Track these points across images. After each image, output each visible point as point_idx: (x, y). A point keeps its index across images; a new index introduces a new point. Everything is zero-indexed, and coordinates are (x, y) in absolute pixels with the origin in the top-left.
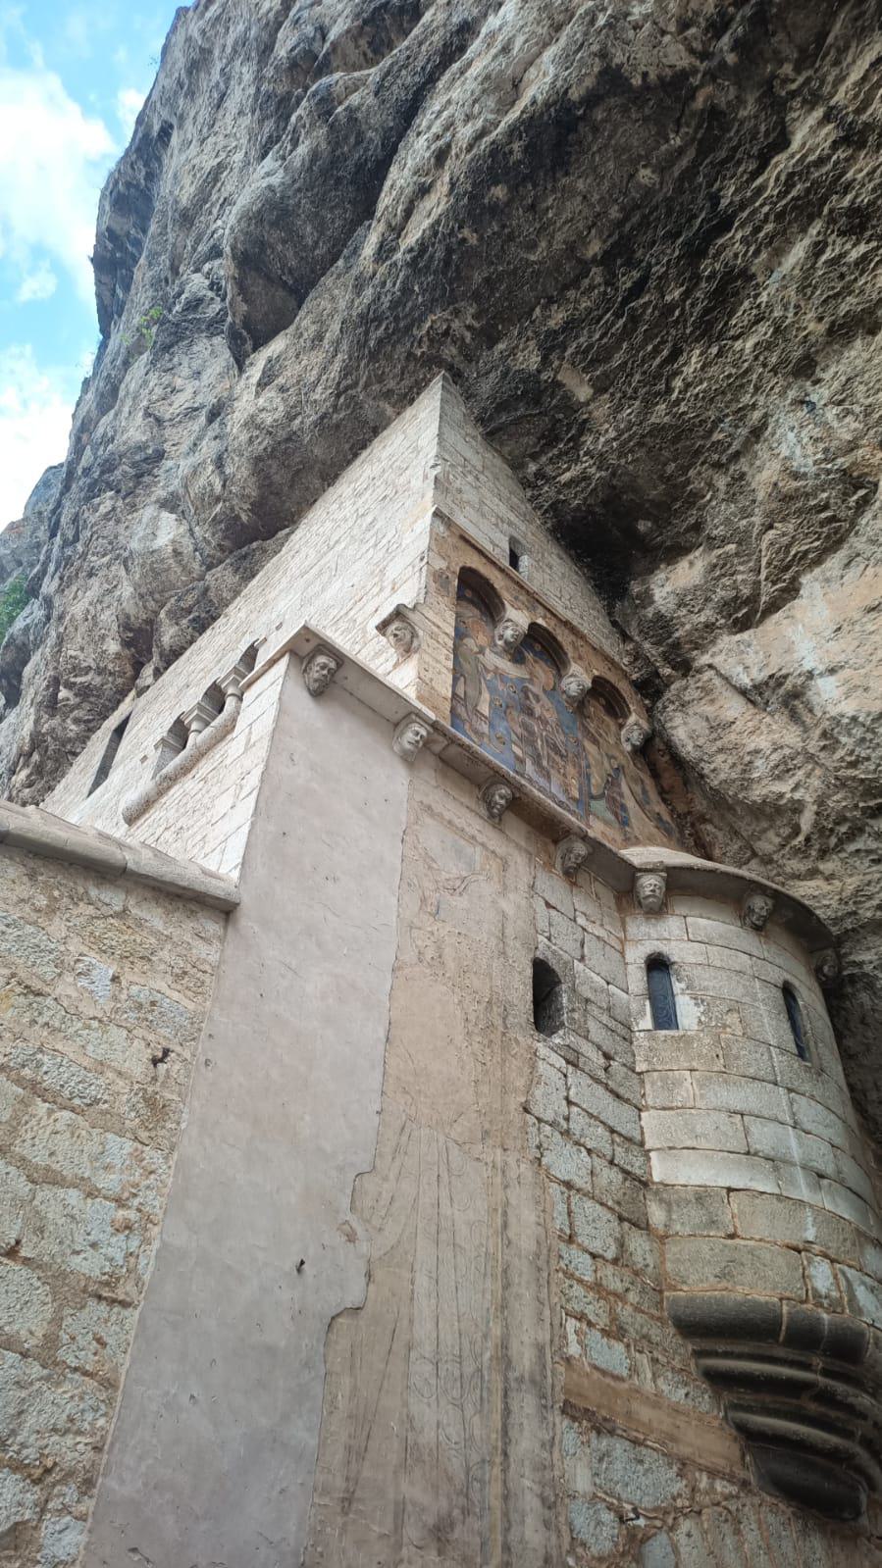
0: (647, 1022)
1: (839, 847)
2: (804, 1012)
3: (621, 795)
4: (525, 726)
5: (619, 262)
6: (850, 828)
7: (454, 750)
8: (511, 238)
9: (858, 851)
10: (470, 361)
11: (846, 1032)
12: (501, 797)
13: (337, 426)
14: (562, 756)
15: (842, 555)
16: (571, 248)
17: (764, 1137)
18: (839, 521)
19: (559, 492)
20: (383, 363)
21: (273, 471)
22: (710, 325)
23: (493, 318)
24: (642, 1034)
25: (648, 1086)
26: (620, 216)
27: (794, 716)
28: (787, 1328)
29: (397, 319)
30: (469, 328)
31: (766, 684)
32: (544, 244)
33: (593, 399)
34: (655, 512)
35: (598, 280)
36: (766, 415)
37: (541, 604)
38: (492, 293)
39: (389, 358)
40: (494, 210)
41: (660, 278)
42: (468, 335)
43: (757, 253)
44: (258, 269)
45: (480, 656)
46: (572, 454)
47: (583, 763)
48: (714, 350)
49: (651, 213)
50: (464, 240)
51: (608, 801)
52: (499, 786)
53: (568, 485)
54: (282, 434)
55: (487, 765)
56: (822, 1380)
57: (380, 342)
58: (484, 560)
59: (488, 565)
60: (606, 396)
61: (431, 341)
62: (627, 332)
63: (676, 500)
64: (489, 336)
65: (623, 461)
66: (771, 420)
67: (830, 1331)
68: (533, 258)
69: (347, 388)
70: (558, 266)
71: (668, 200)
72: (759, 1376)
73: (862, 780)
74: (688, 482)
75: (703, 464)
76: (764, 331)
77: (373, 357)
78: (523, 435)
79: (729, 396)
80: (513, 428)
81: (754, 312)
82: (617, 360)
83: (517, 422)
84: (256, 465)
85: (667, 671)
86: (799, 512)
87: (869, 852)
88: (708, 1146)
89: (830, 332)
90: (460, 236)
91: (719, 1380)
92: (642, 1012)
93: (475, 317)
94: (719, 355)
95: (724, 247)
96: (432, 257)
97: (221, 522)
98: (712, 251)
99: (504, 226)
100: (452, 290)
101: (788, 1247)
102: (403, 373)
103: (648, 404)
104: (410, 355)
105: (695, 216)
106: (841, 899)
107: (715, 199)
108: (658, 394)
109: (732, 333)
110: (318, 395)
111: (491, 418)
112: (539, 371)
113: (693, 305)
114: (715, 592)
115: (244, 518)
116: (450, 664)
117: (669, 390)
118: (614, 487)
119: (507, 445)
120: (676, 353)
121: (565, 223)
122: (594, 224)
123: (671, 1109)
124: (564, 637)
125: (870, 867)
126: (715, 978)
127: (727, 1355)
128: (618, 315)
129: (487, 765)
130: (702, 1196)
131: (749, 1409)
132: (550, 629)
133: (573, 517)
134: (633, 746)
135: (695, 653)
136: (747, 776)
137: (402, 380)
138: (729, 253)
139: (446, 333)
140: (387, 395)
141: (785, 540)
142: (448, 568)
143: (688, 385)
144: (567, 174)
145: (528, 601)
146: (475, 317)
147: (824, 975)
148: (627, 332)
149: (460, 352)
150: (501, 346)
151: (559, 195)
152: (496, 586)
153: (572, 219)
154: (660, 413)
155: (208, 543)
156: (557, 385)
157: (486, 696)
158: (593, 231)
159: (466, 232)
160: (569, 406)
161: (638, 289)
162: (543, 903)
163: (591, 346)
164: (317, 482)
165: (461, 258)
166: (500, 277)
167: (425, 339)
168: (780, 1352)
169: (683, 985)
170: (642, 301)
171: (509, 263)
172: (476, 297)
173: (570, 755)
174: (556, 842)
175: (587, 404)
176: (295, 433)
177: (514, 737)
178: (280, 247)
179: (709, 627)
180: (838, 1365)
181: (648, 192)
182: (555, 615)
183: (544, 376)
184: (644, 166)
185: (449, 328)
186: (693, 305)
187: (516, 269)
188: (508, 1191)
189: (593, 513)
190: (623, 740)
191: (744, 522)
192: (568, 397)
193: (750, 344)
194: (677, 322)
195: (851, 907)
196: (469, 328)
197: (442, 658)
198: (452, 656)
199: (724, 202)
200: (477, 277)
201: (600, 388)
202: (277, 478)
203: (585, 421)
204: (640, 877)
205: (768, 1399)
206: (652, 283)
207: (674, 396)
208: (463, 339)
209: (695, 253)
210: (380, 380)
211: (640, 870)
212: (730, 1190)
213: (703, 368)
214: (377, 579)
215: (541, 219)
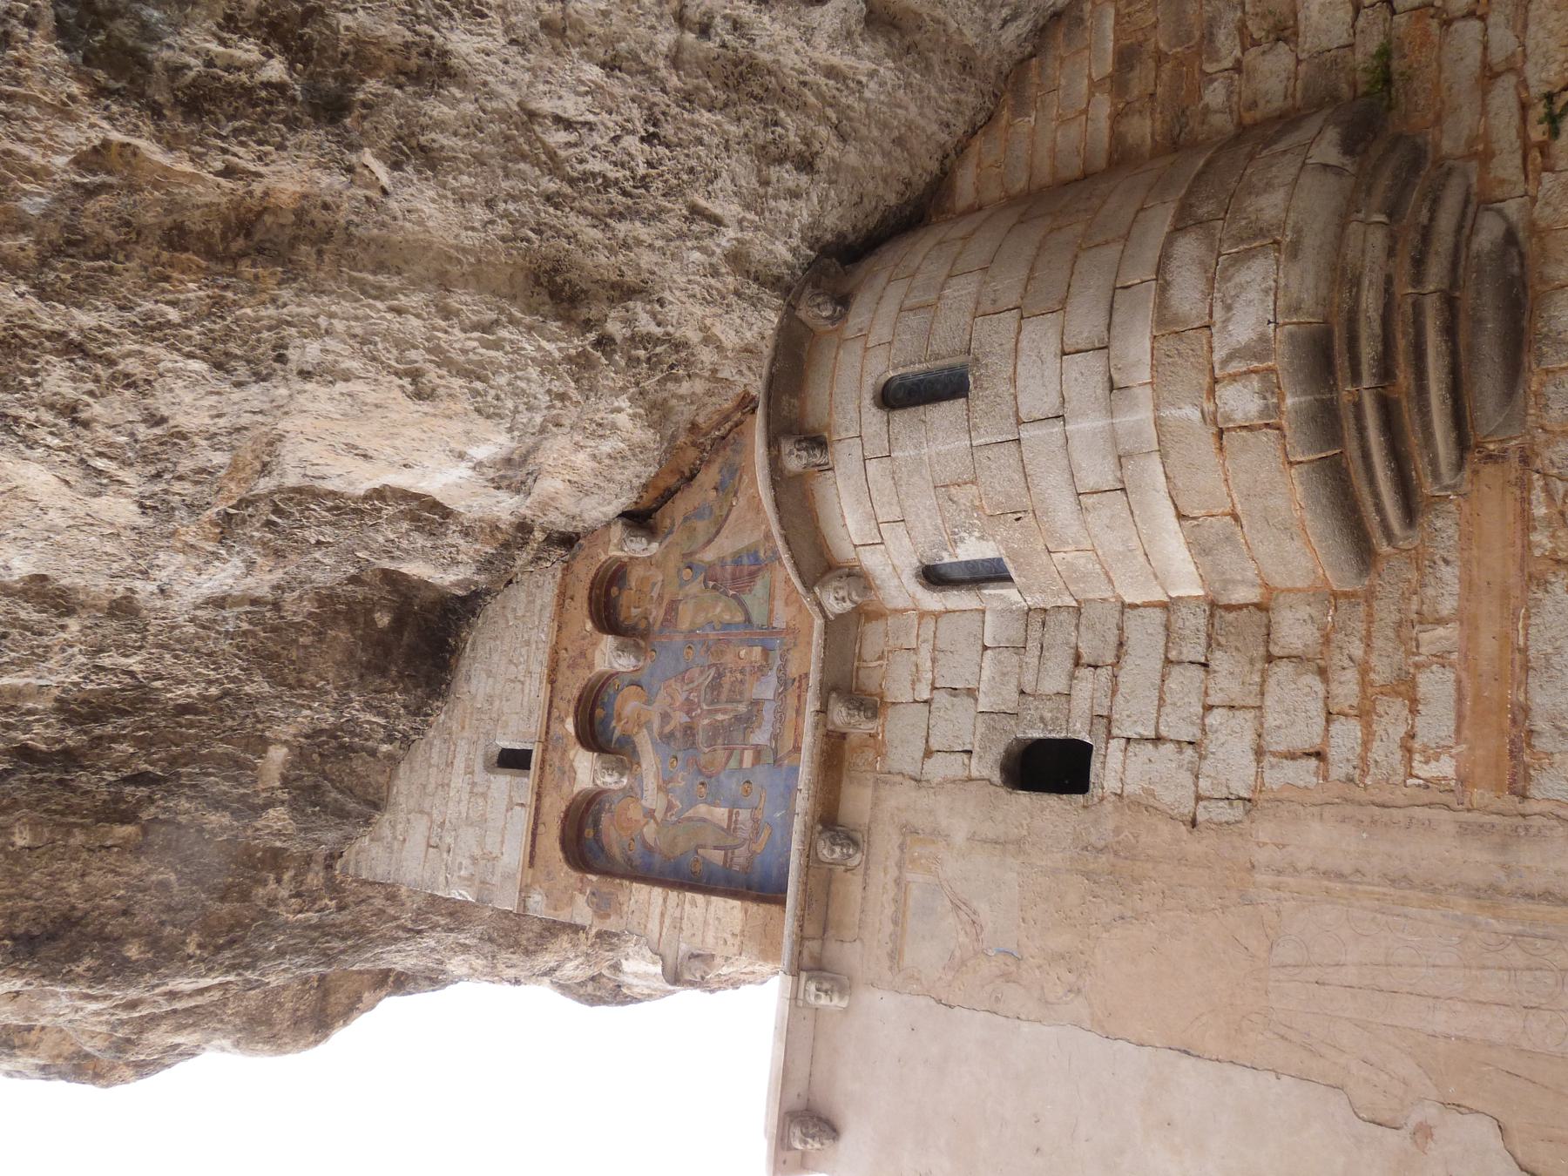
1: (668, 339)
2: (901, 371)
3: (722, 560)
4: (711, 742)
5: (124, 807)
6: (636, 348)
7: (810, 930)
8: (169, 909)
9: (659, 325)
10: (310, 856)
11: (881, 207)
12: (833, 851)
13: (451, 914)
14: (720, 675)
15: (318, 484)
17: (1097, 471)
18: (276, 505)
19: (398, 716)
20: (363, 922)
21: (531, 934)
22: (132, 703)
23: (254, 867)
24: (1028, 599)
25: (1091, 596)
26: (76, 831)
28: (1321, 452)
29: (313, 942)
30: (279, 881)
31: (508, 487)
32: (154, 877)
33: (278, 741)
34: (361, 620)
35: (153, 810)
37: (548, 727)
38: (232, 885)
39: (355, 921)
41: (117, 770)
42: (286, 877)
43: (30, 712)
44: (323, 1010)
45: (659, 815)
47: (712, 635)
48: (158, 684)
49: (55, 812)
50: (200, 946)
51: (741, 590)
52: (820, 856)
54: (488, 947)
55: (806, 884)
56: (1367, 381)
58: (541, 829)
59: (543, 818)
60: (267, 734)
61: (314, 902)
63: (337, 612)
65: (329, 688)
67: (1305, 393)
68: (173, 877)
69: (409, 930)
70: (165, 848)
72: (1392, 470)
73: (577, 381)
74: (311, 615)
75: (282, 617)
76: (106, 660)
78: (359, 777)
79: (197, 643)
80: (358, 791)
81: (93, 677)
82: (221, 748)
83: (349, 791)
84: (535, 952)
85: (539, 535)
87: (654, 315)
88: (1135, 538)
89: (70, 612)
90: (198, 952)
91: (1410, 510)
92: (1001, 598)
93: (264, 883)
94: (160, 677)
95: (46, 740)
97: (611, 944)
98: (58, 747)
99: (162, 923)
100: (254, 920)
101: (1221, 449)
102: (363, 901)
103: (253, 701)
104: (340, 908)
106: (727, 313)
108: (238, 700)
109: (128, 680)
111: (360, 815)
112: (283, 803)
113: (124, 727)
114: (423, 547)
116: (700, 898)
118: (361, 677)
119: (377, 782)
121: (119, 874)
122: (102, 847)
123: (1107, 574)
124: (572, 686)
125: (671, 303)
126: (917, 515)
127: (1379, 509)
129: (806, 884)
131: (1434, 462)
132: (572, 710)
133: (417, 686)
134: (649, 543)
135: (503, 526)
136: (628, 453)
137: (370, 897)
139: (298, 895)
142: (582, 891)
143: (210, 682)
144: (73, 908)
145: (555, 748)
146: (264, 883)
147: (835, 311)
148: (191, 758)
149: (309, 870)
150: (278, 844)
151: (97, 900)
152: (564, 808)
153: (112, 871)
154: (258, 686)
156: (285, 780)
157: (702, 809)
158: (109, 843)
159: (191, 948)
160: (300, 756)
161: (139, 779)
162: (929, 763)
165: (217, 935)
167: (316, 907)
168: (1352, 447)
169: (945, 554)
170: (150, 768)
171: (193, 892)
172: (245, 896)
173: (712, 660)
174: (843, 736)
175: (286, 743)
176: (480, 939)
177: (733, 764)
180: (1341, 362)
181: (34, 825)
182: (551, 702)
183: (286, 796)
184: (13, 845)
185: (291, 896)
186: (124, 727)
187: (195, 882)
188: (1300, 865)
189: (401, 676)
190: (647, 554)
193: (131, 661)
194: (150, 728)
195: (732, 299)
196: (279, 881)
197: (698, 912)
198: (689, 895)
201: (263, 743)
203: (307, 737)
204: (832, 613)
205: (1414, 440)
206: (126, 772)
208: (294, 877)
209: (70, 758)
211: (825, 617)
212: (1181, 517)
213: (183, 682)
215: (131, 898)
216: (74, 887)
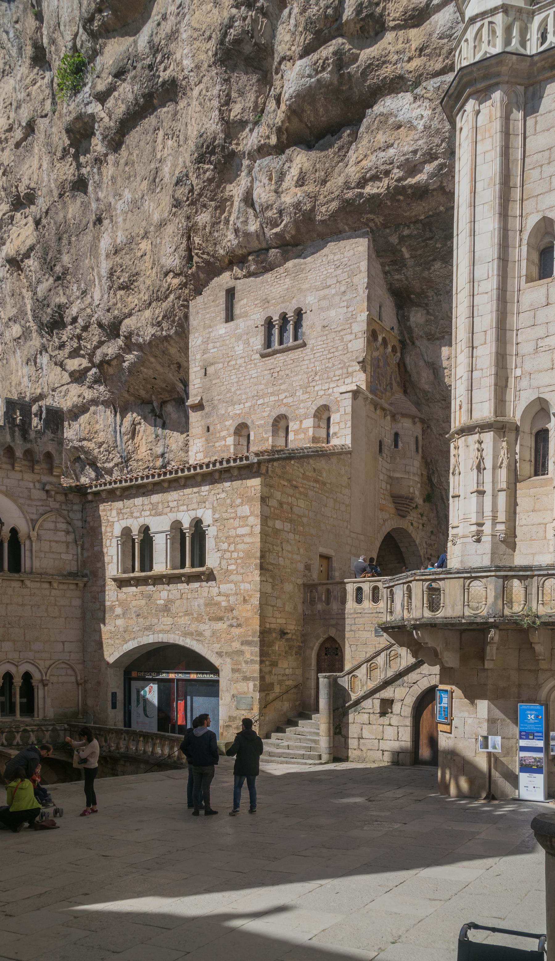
16: (416, 216)
46: (399, 271)
115: (288, 238)
128: (423, 241)
156: (401, 250)
178: (309, 112)
192: (402, 255)
206: (434, 239)
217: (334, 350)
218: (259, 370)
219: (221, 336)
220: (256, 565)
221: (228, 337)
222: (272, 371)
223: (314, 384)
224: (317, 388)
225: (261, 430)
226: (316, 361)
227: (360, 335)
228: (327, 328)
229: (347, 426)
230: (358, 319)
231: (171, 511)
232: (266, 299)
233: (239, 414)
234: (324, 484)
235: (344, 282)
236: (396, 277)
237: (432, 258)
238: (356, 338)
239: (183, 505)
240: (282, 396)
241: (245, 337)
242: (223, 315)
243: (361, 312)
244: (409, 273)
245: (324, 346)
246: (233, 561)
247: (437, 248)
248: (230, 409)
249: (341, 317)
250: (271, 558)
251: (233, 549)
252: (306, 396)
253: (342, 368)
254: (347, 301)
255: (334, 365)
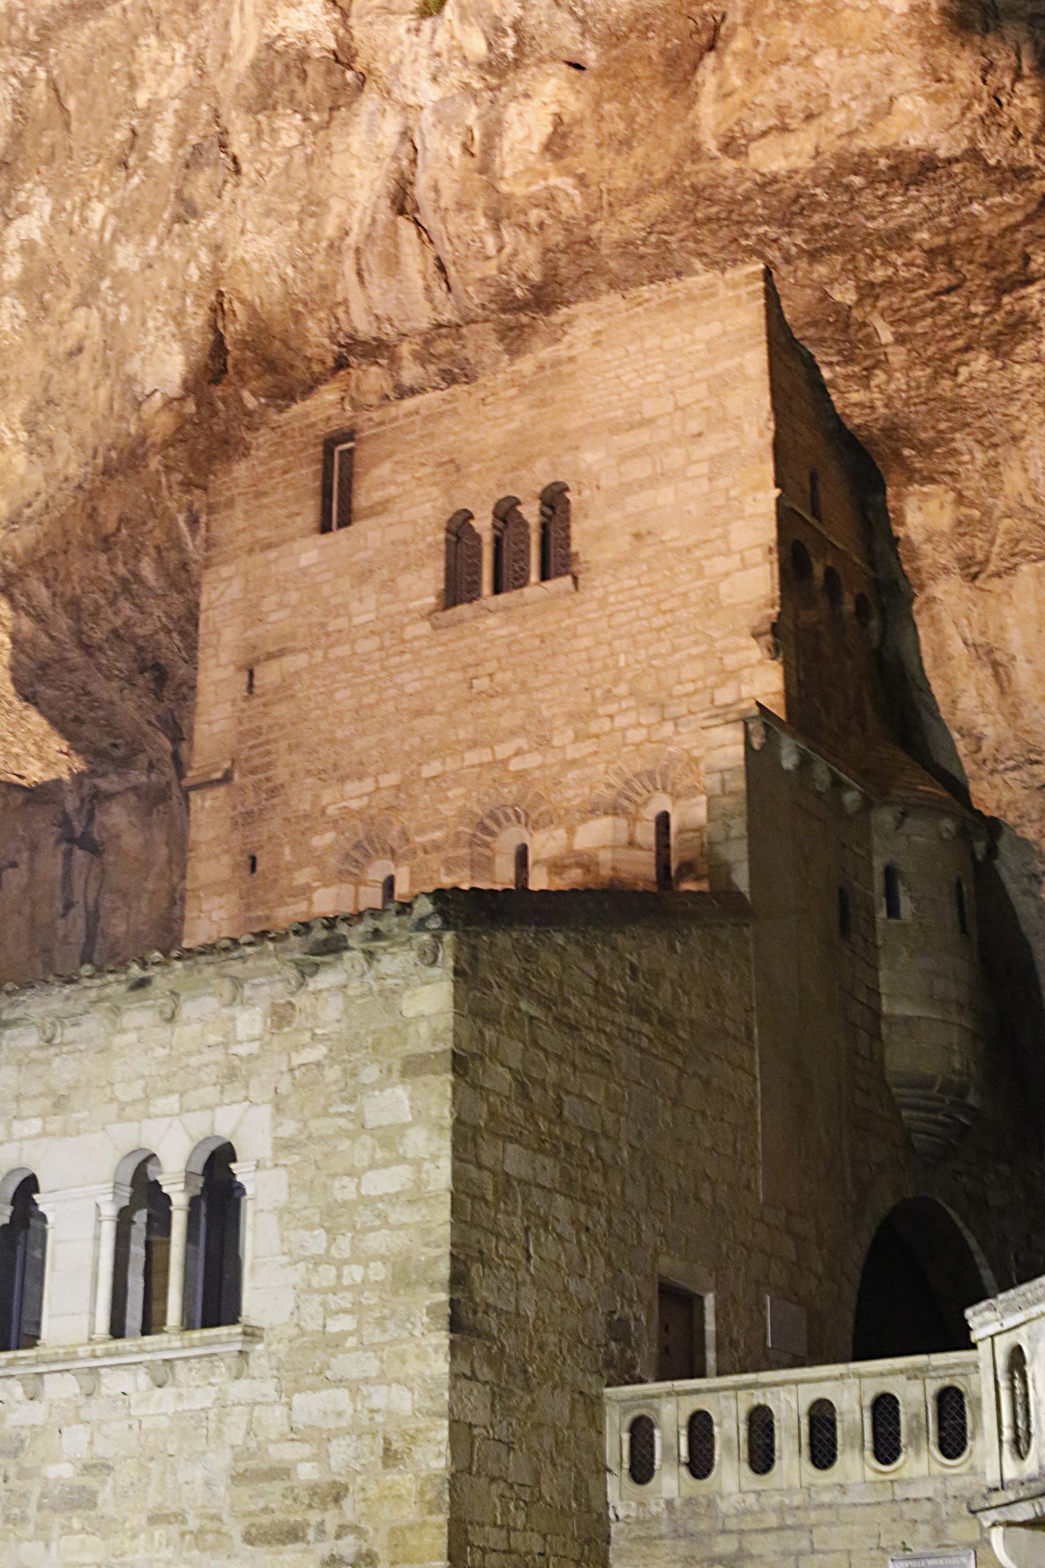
0: (882, 913)
13: (642, 257)
27: (996, 675)
36: (1025, 432)
40: (848, 188)
53: (855, 405)
54: (579, 233)
57: (709, 219)
60: (903, 350)
62: (932, 313)
64: (814, 256)
66: (1028, 438)
71: (991, 240)
74: (953, 440)
77: (697, 223)
82: (920, 328)
84: (544, 254)
86: (1034, 521)
96: (780, 191)
98: (1015, 295)
105: (1008, 262)
107: (1027, 259)
110: (627, 215)
115: (518, 292)
117: (956, 373)
120: (967, 348)
128: (931, 297)
130: (907, 1020)
138: (1026, 303)
139: (775, 241)
140: (702, 255)
141: (1017, 535)
143: (971, 378)
148: (932, 313)
155: (471, 298)
156: (864, 325)
160: (869, 341)
163: (900, 309)
164: (604, 287)
166: (837, 225)
175: (886, 345)
179: (946, 570)
191: (990, 500)
194: (974, 327)
199: (1033, 266)
200: (817, 219)
201: (901, 339)
202: (563, 271)
206: (963, 292)
207: (961, 379)
209: (1002, 288)
210: (697, 241)
214: (719, 530)
216: (926, 200)
217: (675, 602)
218: (428, 671)
219: (304, 572)
220: (431, 1311)
221: (329, 576)
222: (472, 672)
223: (612, 708)
224: (620, 721)
225: (434, 860)
226: (615, 638)
227: (758, 555)
228: (649, 540)
229: (734, 833)
230: (749, 510)
231: (120, 1118)
232: (452, 461)
233: (360, 812)
234: (667, 1023)
235: (696, 409)
236: (855, 397)
237: (960, 343)
238: (744, 566)
239: (168, 1092)
240: (503, 751)
241: (385, 574)
242: (310, 513)
243: (755, 489)
244: (893, 386)
245: (640, 592)
246: (345, 1300)
247: (975, 315)
248: (327, 797)
249: (692, 507)
250: (484, 1291)
251: (347, 1254)
252: (588, 747)
253: (702, 657)
254: (712, 459)
255: (675, 649)
